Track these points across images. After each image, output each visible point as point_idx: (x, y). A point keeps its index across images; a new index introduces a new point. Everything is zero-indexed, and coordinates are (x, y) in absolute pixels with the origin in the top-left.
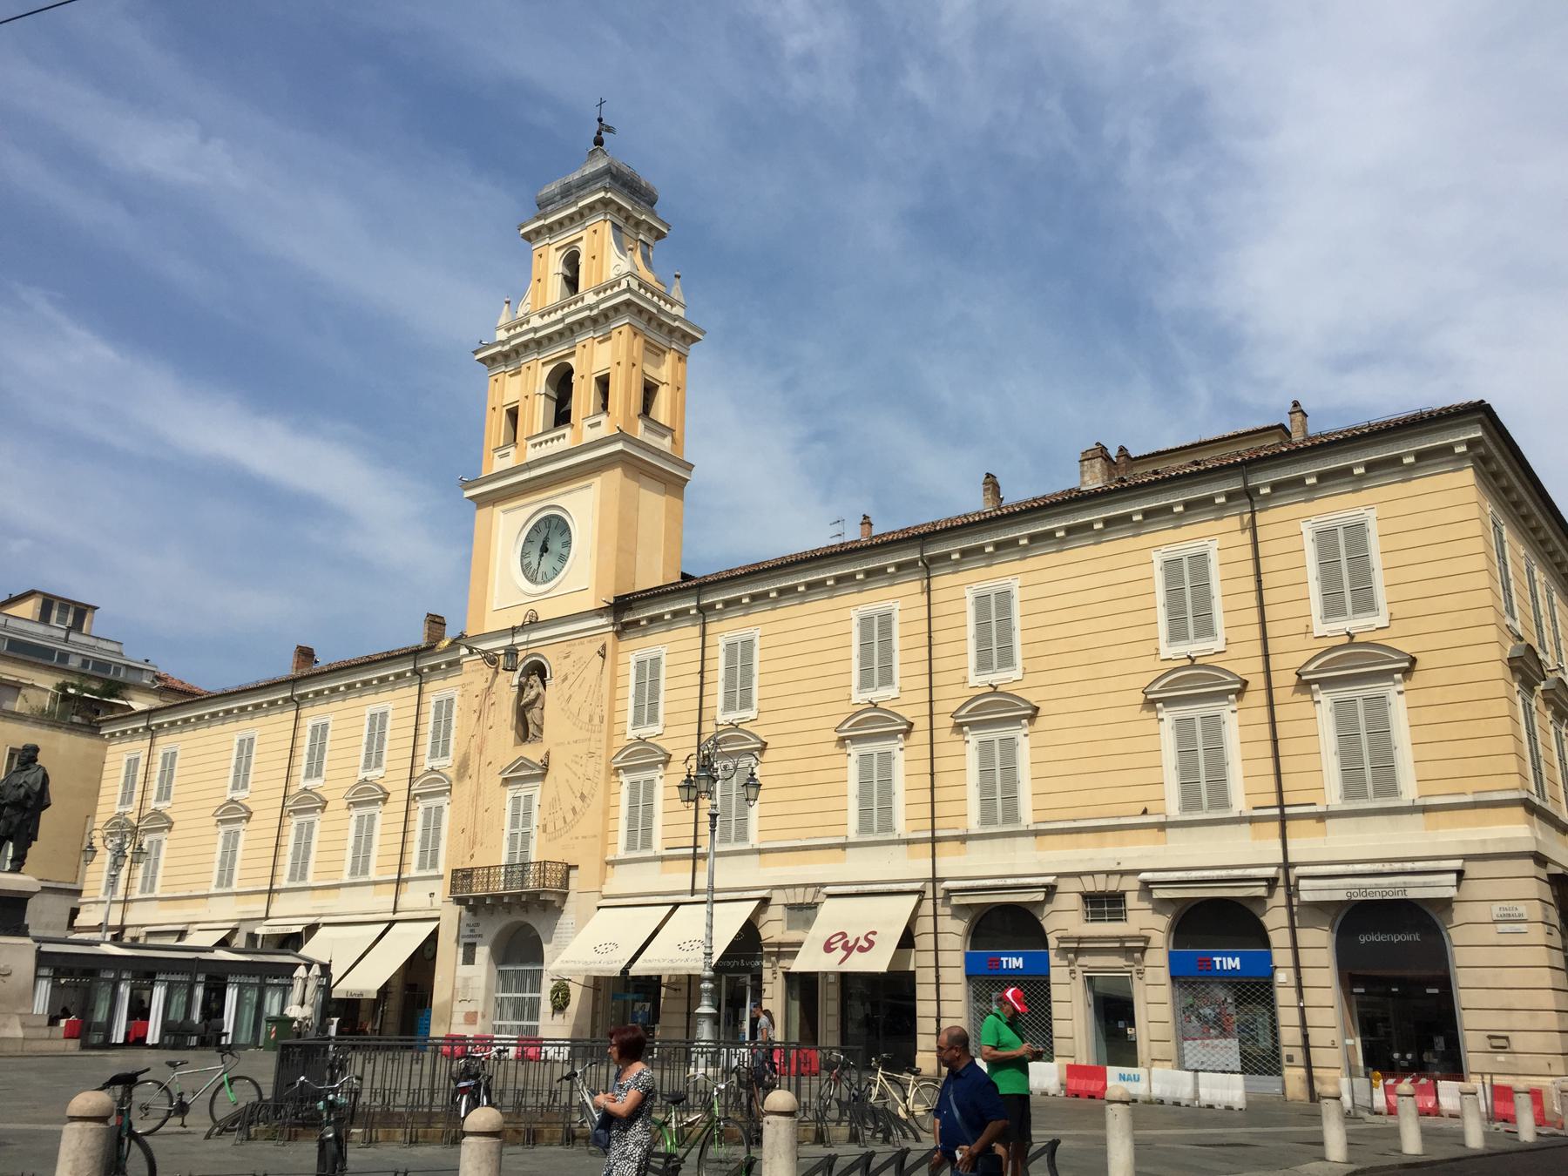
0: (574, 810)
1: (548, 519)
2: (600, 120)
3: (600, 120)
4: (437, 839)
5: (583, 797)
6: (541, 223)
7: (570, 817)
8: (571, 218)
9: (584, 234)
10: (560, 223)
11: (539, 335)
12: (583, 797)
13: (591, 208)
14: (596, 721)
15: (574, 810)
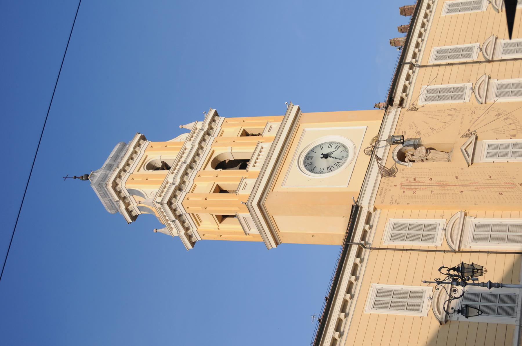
0: (505, 119)
1: (306, 166)
2: (75, 177)
3: (75, 177)
4: (501, 227)
5: (499, 115)
6: (118, 170)
7: (509, 121)
8: (131, 158)
9: (147, 153)
10: (128, 164)
11: (188, 162)
12: (499, 115)
13: (138, 145)
14: (452, 112)
15: (505, 119)
